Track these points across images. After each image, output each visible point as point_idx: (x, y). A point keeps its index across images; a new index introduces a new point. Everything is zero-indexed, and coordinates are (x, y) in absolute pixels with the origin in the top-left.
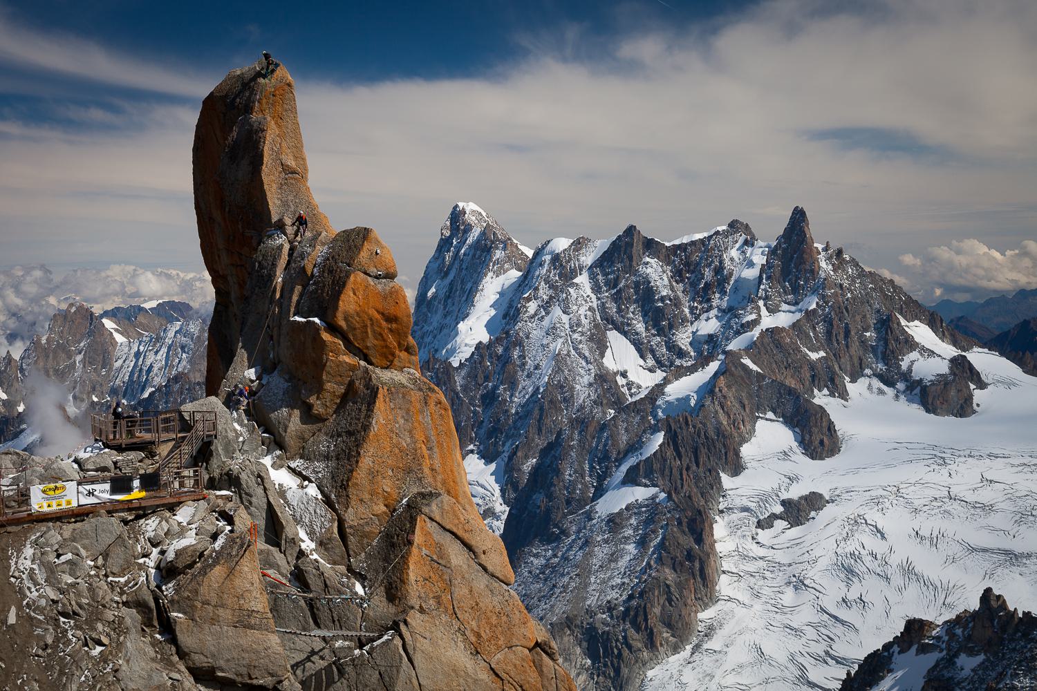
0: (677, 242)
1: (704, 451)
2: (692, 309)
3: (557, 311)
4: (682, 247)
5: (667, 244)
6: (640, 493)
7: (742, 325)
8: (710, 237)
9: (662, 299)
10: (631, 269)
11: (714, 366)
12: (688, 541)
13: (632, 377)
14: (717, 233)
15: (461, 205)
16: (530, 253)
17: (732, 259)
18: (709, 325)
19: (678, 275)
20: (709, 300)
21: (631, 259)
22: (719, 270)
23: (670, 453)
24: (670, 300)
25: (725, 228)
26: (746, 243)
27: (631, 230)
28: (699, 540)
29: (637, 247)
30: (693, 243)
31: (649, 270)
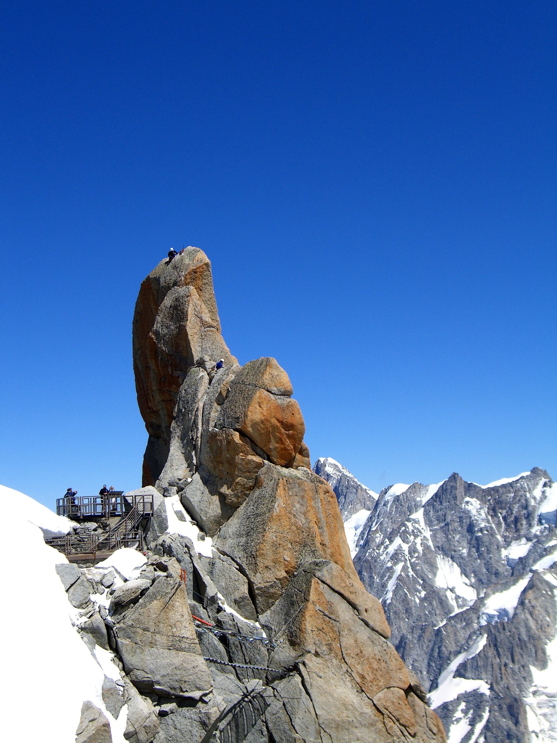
0: (492, 485)
1: (517, 650)
2: (505, 537)
3: (398, 541)
4: (495, 489)
5: (484, 487)
6: (468, 685)
7: (545, 550)
8: (518, 480)
9: (481, 530)
10: (455, 507)
11: (523, 583)
12: (506, 723)
13: (459, 592)
14: (522, 478)
15: (322, 460)
16: (376, 496)
17: (535, 498)
18: (518, 550)
19: (493, 511)
20: (517, 530)
21: (455, 498)
22: (526, 507)
23: (491, 652)
24: (487, 531)
25: (528, 473)
26: (545, 485)
27: (454, 477)
28: (517, 723)
29: (460, 491)
30: (504, 486)
31: (469, 507)
